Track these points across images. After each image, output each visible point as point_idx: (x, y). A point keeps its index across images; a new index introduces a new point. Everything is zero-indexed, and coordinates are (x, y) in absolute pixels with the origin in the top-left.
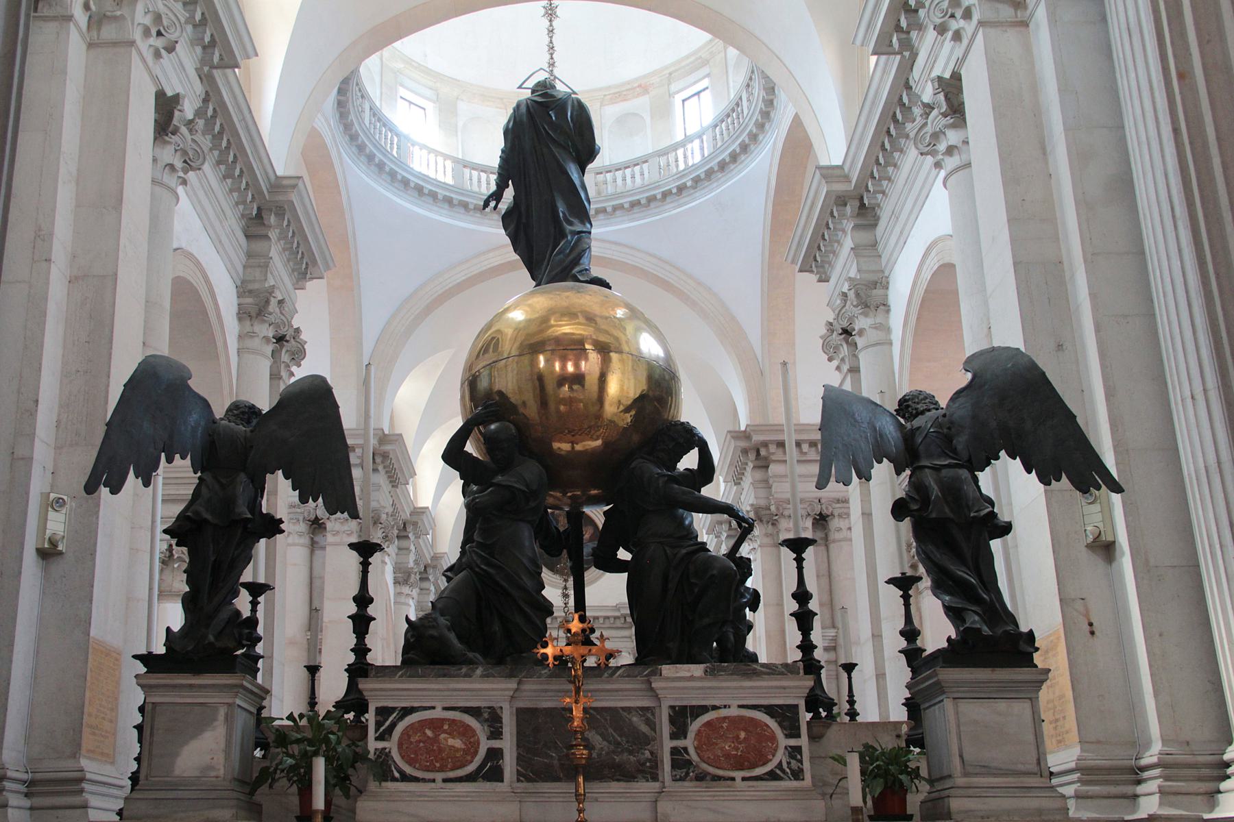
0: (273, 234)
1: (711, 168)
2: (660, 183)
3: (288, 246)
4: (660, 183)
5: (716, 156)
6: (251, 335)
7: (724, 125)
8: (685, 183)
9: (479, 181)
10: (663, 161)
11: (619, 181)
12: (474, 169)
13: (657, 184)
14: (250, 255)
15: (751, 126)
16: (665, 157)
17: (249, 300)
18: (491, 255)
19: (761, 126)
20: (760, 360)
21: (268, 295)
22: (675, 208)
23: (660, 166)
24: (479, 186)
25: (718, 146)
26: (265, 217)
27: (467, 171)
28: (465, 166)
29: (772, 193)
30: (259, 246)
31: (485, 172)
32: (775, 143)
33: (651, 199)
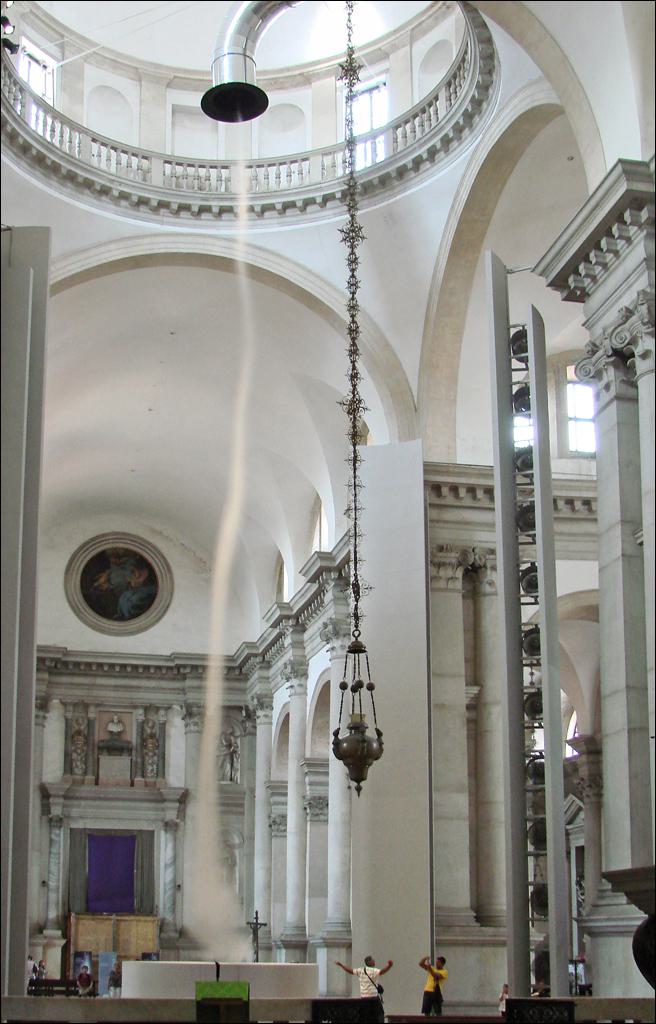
2: (323, 185)
4: (323, 185)
5: (396, 161)
7: (408, 126)
9: (109, 159)
10: (328, 160)
11: (272, 177)
12: (104, 144)
15: (448, 130)
16: (330, 157)
18: (113, 246)
19: (459, 130)
20: (415, 393)
23: (323, 166)
24: (109, 165)
25: (408, 144)
27: (95, 146)
28: (94, 140)
29: (460, 208)
31: (115, 149)
32: (476, 150)
33: (308, 203)
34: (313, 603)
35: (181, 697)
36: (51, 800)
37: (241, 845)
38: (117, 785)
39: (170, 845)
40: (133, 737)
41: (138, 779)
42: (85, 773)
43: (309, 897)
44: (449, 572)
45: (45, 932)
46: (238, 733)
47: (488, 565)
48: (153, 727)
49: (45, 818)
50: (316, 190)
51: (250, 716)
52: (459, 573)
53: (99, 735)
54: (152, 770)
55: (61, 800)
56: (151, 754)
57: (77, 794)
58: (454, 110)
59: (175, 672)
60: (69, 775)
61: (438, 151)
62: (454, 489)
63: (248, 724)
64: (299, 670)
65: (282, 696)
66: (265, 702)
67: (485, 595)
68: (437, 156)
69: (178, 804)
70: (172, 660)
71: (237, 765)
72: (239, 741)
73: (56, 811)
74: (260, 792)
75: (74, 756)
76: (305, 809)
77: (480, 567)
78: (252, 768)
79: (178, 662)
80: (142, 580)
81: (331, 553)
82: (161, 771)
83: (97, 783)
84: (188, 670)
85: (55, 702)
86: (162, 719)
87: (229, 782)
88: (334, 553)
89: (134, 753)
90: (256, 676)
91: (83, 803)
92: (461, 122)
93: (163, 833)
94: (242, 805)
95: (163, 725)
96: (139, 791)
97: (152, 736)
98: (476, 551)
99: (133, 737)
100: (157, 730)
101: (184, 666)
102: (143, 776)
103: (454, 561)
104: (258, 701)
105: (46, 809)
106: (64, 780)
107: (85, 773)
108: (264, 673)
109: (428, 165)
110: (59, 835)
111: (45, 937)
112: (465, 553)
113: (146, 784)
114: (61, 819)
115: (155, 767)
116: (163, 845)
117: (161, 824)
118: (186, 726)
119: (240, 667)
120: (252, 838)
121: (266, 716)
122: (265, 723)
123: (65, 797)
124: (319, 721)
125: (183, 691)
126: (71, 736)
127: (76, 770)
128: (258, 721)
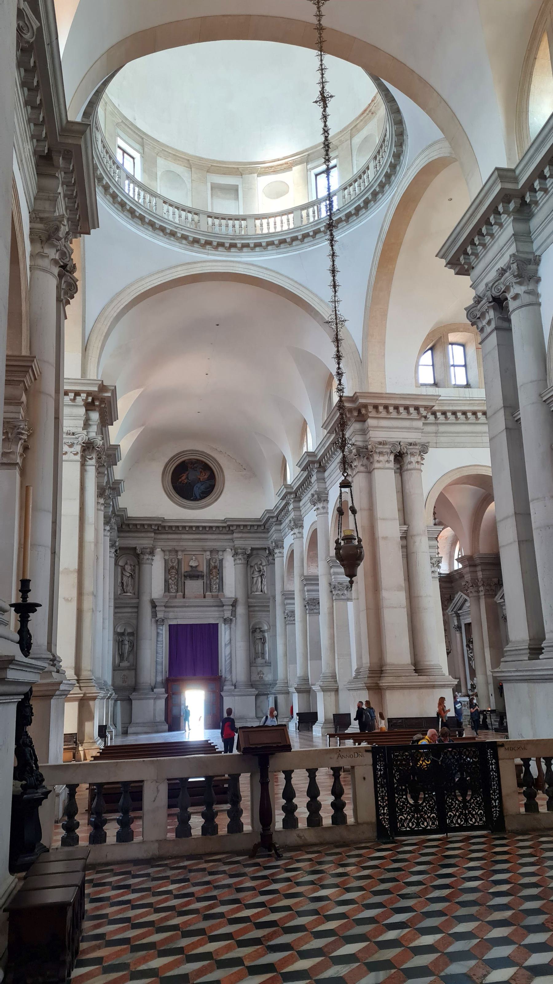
0: (60, 175)
1: (340, 218)
2: (301, 228)
3: (69, 193)
4: (301, 228)
6: (42, 256)
8: (319, 229)
13: (299, 228)
14: (40, 189)
17: (40, 226)
19: (382, 186)
20: (360, 353)
21: (58, 223)
22: (310, 246)
25: (352, 198)
26: (54, 157)
29: (384, 236)
30: (48, 183)
33: (294, 239)
34: (305, 483)
35: (231, 544)
36: (157, 609)
37: (268, 630)
38: (196, 597)
39: (228, 633)
40: (204, 568)
41: (208, 593)
42: (177, 591)
43: (310, 660)
44: (385, 458)
45: (155, 690)
46: (264, 564)
47: (409, 453)
48: (215, 562)
49: (153, 620)
50: (298, 231)
51: (271, 553)
52: (392, 458)
53: (184, 568)
54: (216, 588)
55: (164, 608)
56: (215, 578)
57: (172, 605)
58: (382, 167)
59: (227, 529)
60: (167, 593)
61: (370, 201)
62: (386, 407)
63: (270, 558)
64: (298, 524)
65: (289, 540)
66: (279, 544)
67: (407, 470)
68: (369, 205)
69: (231, 607)
70: (226, 522)
71: (265, 582)
72: (265, 568)
73: (160, 615)
74: (279, 598)
75: (170, 581)
76: (305, 606)
77: (404, 453)
78: (274, 584)
79: (229, 523)
80: (206, 477)
81: (314, 453)
82: (221, 588)
83: (184, 597)
84: (235, 528)
85: (158, 550)
86: (221, 557)
87: (261, 593)
88: (316, 452)
89: (205, 578)
90: (274, 529)
91: (176, 609)
92: (384, 180)
93: (223, 625)
94: (268, 606)
95: (221, 561)
96: (209, 600)
97: (215, 567)
98: (402, 444)
99: (204, 568)
100: (218, 563)
101: (232, 526)
102: (211, 592)
103: (388, 451)
104: (275, 543)
105: (154, 614)
106: (164, 596)
107: (177, 591)
108: (278, 527)
109: (364, 211)
110: (162, 630)
111: (155, 693)
112: (393, 444)
113: (212, 596)
114: (163, 620)
115: (217, 586)
116: (223, 633)
117: (222, 620)
118: (235, 561)
119: (264, 525)
120: (275, 626)
121: (280, 552)
122: (280, 557)
123: (166, 607)
124: (311, 553)
125: (232, 540)
126: (168, 570)
127: (171, 590)
128: (276, 556)
